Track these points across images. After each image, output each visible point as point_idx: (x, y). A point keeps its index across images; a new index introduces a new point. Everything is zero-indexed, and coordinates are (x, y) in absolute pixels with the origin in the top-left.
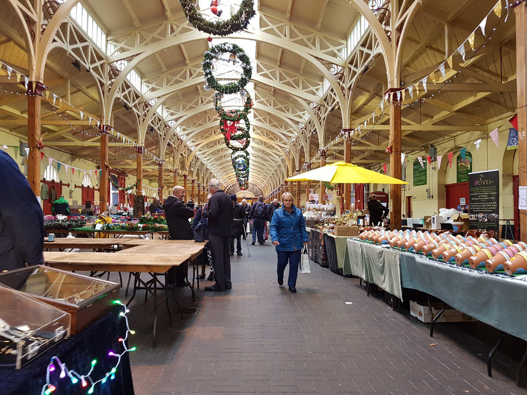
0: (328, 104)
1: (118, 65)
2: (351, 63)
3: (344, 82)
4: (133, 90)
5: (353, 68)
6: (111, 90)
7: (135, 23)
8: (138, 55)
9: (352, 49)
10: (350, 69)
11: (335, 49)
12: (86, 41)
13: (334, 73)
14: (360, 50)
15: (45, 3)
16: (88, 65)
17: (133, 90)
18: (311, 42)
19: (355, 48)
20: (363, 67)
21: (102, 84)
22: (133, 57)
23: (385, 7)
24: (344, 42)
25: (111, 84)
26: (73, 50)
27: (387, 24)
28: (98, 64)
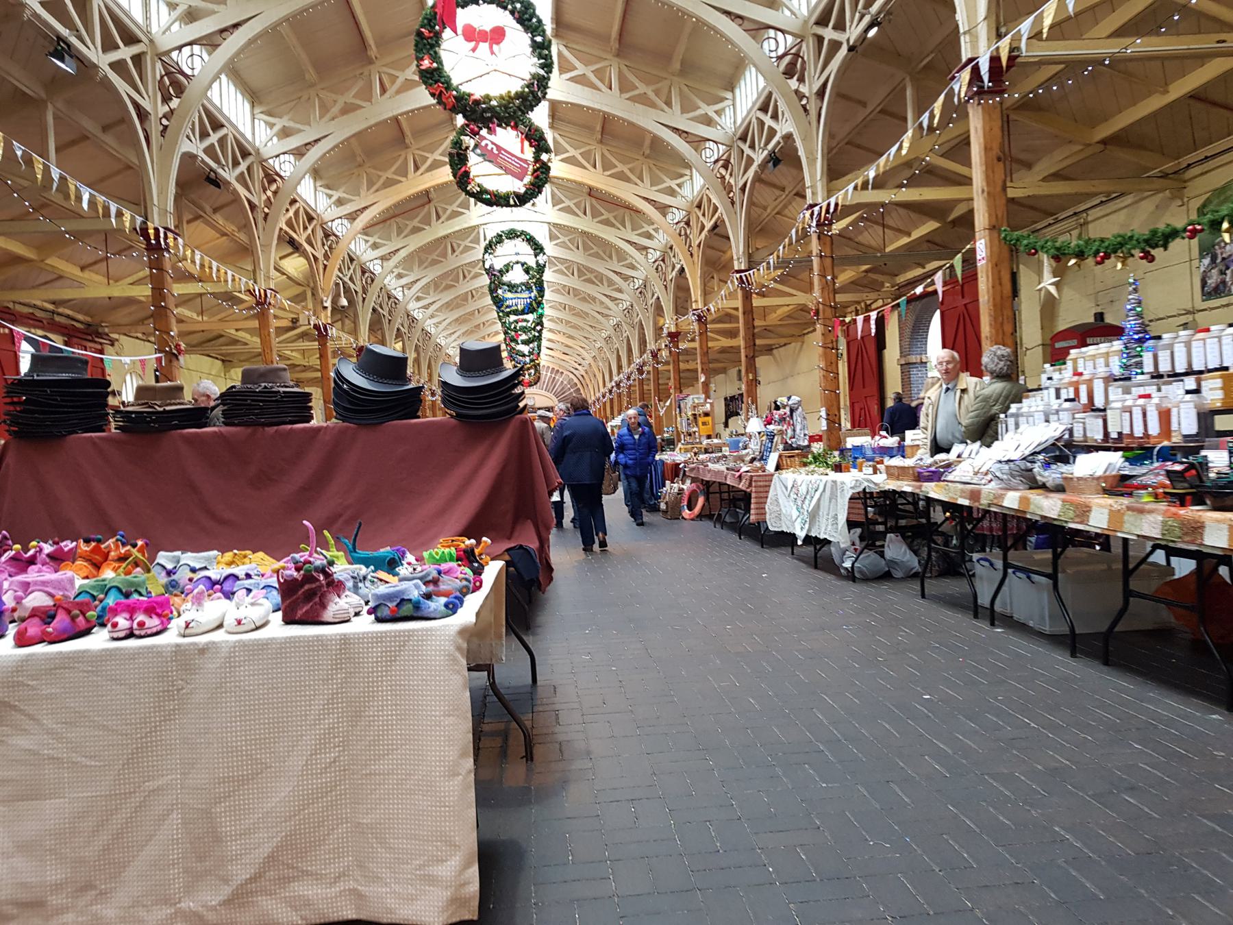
0: (704, 215)
1: (275, 164)
2: (743, 138)
3: (731, 175)
4: (301, 209)
5: (747, 151)
6: (269, 217)
7: (307, 76)
8: (316, 141)
9: (745, 113)
10: (743, 152)
11: (710, 111)
12: (223, 126)
13: (713, 160)
14: (758, 118)
15: (162, 77)
16: (230, 175)
17: (301, 209)
18: (664, 98)
19: (749, 113)
20: (766, 152)
21: (253, 207)
22: (308, 147)
23: (793, 51)
24: (729, 95)
25: (269, 203)
26: (206, 151)
27: (801, 80)
28: (243, 167)
